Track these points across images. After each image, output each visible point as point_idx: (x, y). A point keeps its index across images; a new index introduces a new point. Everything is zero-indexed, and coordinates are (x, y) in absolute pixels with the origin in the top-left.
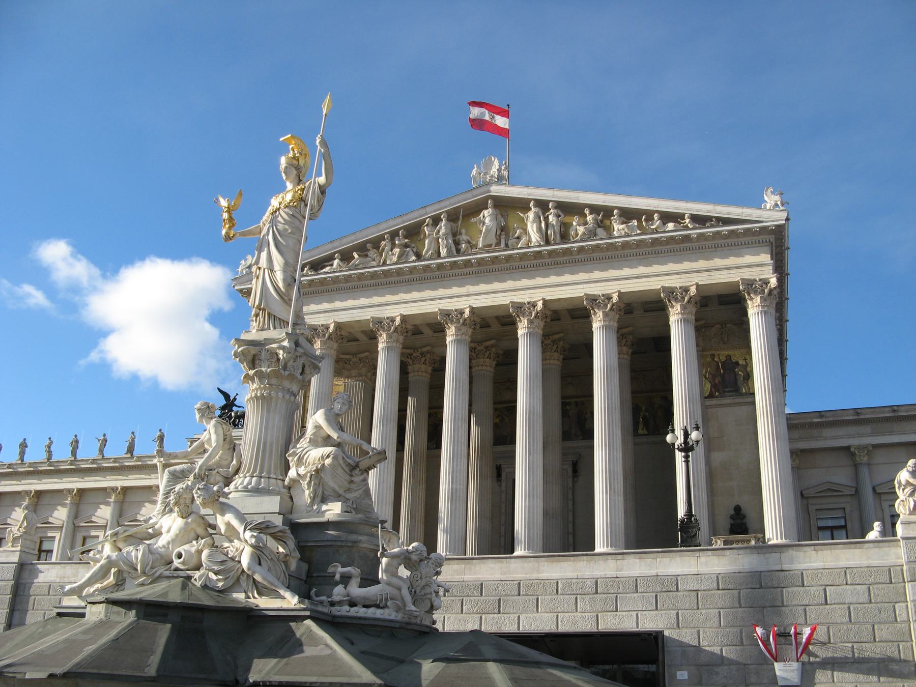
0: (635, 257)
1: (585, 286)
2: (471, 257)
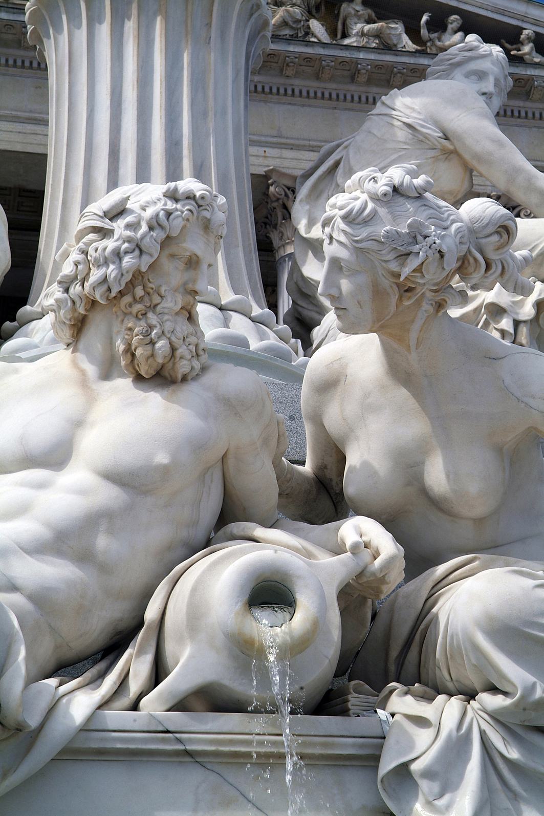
1: (271, 152)
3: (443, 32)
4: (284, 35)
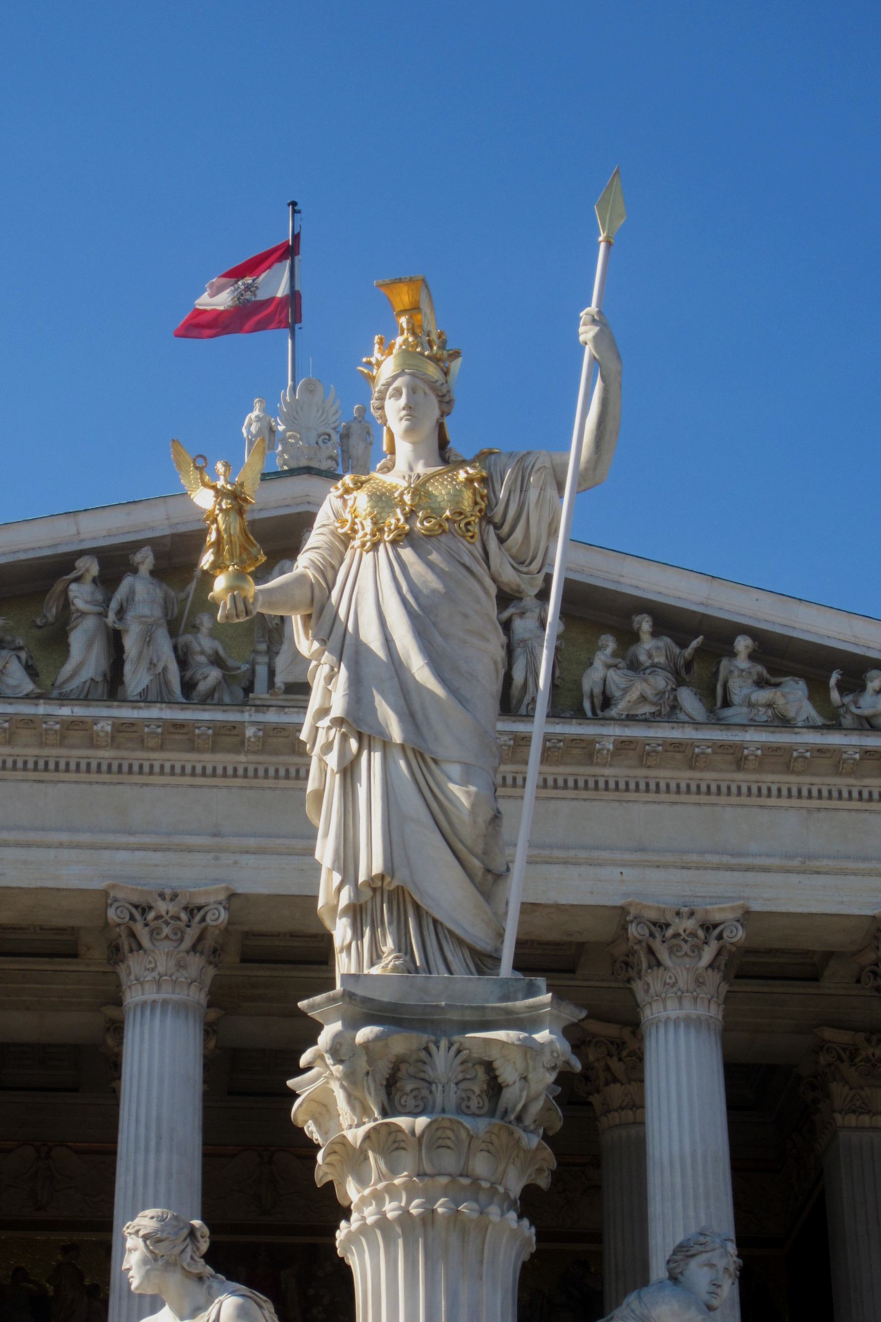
0: (795, 802)
2: (246, 717)
3: (861, 691)
4: (642, 715)
